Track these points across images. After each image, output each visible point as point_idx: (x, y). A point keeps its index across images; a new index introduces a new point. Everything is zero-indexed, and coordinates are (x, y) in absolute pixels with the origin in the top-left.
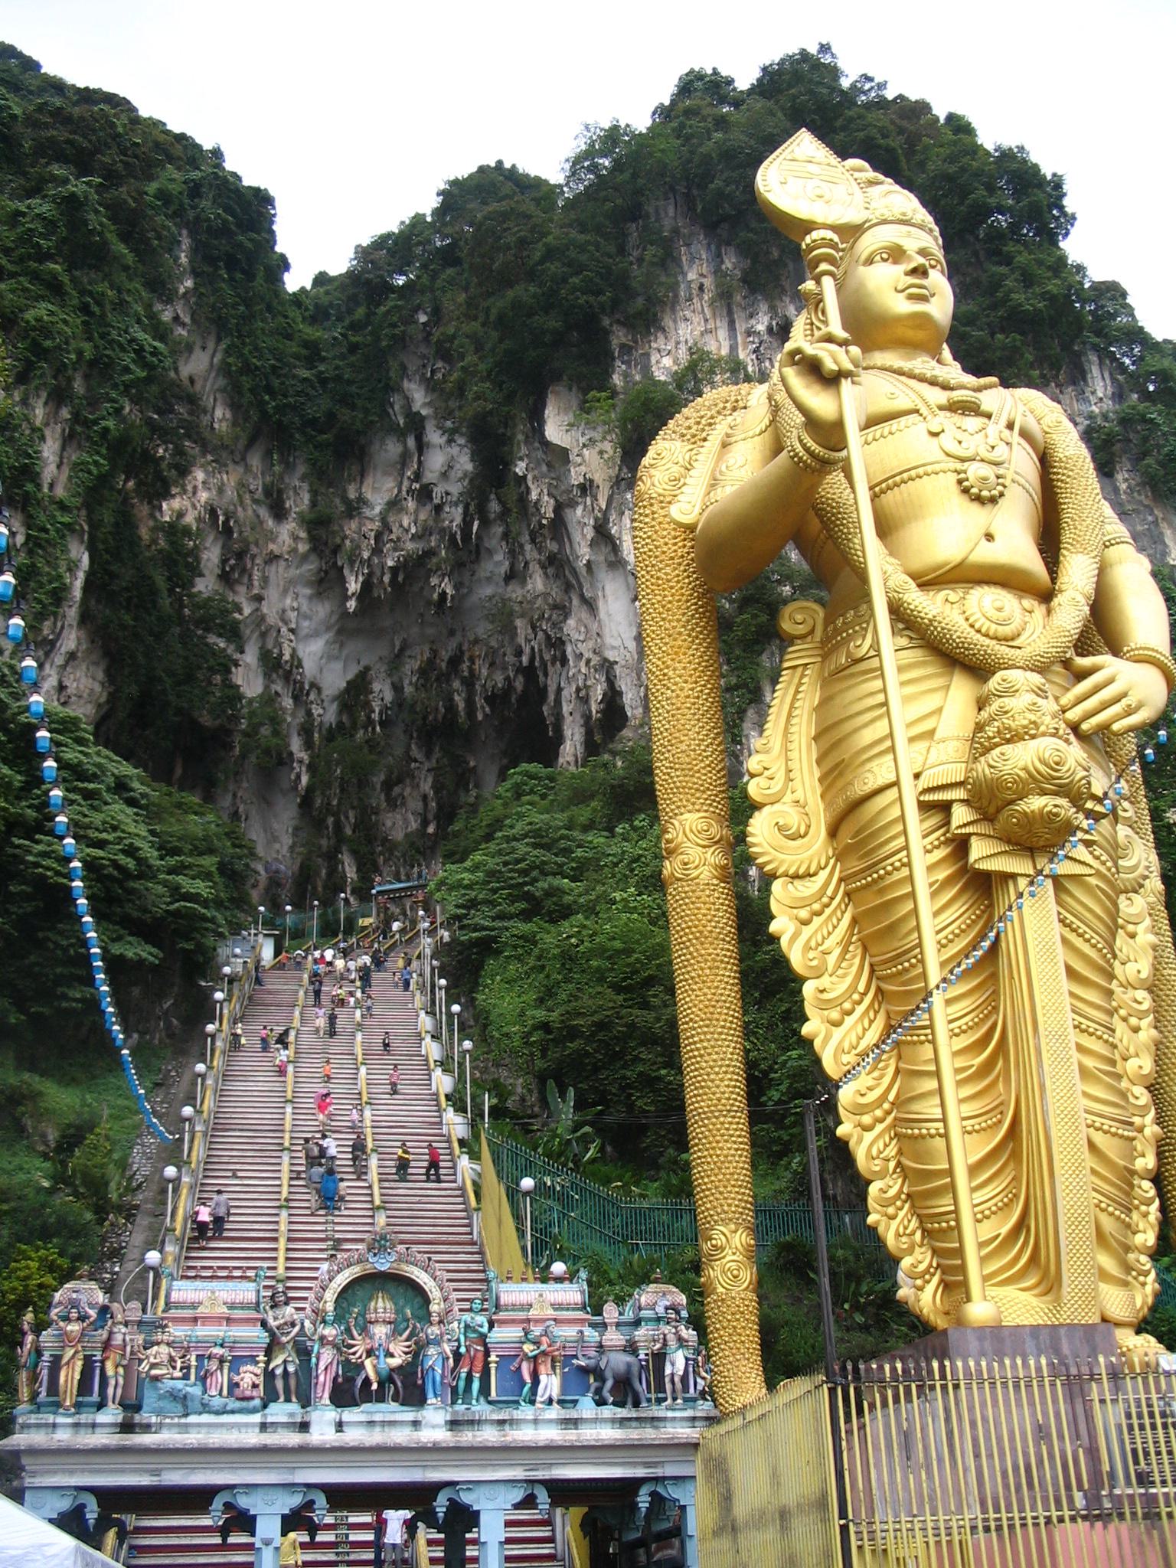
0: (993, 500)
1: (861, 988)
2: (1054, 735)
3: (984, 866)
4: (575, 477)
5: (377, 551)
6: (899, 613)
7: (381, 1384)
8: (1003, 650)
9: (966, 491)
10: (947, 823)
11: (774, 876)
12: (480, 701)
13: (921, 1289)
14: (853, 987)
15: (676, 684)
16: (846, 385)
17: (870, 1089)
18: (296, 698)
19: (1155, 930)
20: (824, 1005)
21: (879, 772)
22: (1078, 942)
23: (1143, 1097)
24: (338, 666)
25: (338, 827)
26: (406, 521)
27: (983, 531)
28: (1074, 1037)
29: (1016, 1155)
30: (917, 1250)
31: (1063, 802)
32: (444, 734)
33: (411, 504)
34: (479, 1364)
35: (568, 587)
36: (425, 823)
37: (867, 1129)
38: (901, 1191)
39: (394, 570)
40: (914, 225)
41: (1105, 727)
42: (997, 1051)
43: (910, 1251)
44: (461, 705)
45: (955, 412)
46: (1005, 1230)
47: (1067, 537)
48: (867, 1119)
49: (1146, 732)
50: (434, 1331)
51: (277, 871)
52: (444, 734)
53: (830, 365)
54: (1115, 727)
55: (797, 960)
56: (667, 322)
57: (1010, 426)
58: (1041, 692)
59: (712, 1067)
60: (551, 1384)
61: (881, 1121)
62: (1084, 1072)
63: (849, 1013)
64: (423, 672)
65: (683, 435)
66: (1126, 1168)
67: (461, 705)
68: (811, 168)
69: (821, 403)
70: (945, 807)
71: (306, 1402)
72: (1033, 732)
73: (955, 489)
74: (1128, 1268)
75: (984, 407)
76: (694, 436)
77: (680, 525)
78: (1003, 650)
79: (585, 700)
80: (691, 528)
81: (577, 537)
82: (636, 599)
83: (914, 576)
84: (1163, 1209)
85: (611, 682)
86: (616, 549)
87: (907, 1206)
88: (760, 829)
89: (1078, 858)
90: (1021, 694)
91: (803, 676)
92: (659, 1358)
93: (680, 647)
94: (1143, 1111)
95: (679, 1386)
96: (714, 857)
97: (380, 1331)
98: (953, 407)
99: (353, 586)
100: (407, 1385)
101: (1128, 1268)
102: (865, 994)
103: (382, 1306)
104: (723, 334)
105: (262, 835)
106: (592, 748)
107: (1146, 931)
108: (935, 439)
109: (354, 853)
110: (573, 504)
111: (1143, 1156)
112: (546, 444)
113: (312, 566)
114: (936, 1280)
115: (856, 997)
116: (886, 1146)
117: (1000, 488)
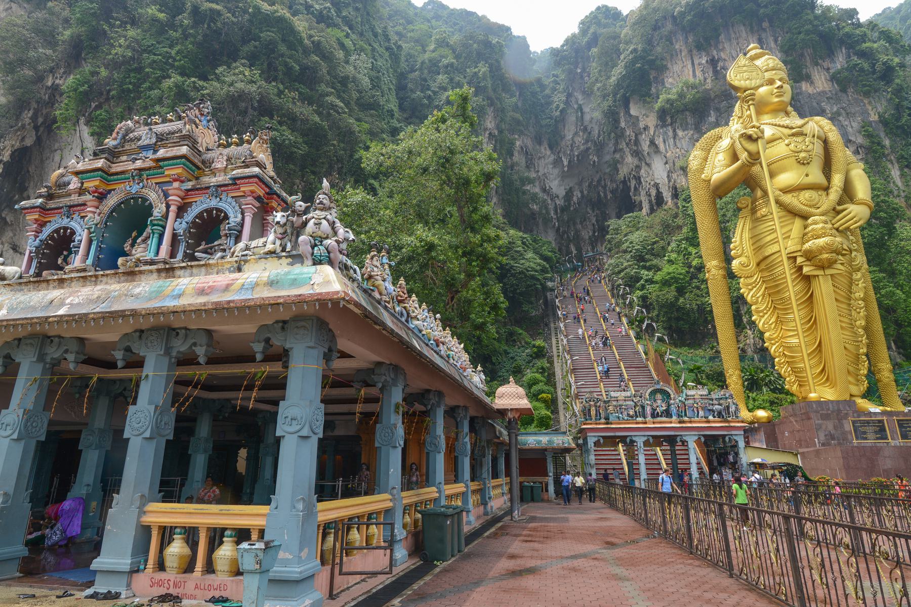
0: (808, 163)
4: (641, 125)
5: (572, 150)
6: (777, 202)
8: (813, 210)
10: (795, 261)
12: (608, 193)
14: (767, 306)
16: (760, 141)
18: (551, 200)
20: (758, 312)
21: (774, 248)
24: (563, 188)
25: (568, 237)
26: (579, 140)
28: (838, 318)
29: (820, 351)
31: (834, 255)
32: (599, 204)
33: (581, 134)
35: (640, 160)
36: (594, 232)
39: (578, 156)
41: (848, 229)
44: (602, 195)
47: (833, 168)
49: (862, 229)
50: (672, 402)
52: (599, 204)
53: (755, 136)
55: (749, 299)
56: (669, 66)
57: (814, 136)
58: (826, 222)
60: (701, 413)
62: (842, 328)
64: (589, 186)
67: (602, 195)
68: (745, 68)
70: (795, 258)
71: (645, 417)
74: (858, 381)
78: (813, 210)
79: (650, 196)
81: (643, 143)
82: (666, 163)
83: (781, 190)
84: (869, 363)
85: (658, 189)
86: (657, 147)
88: (735, 264)
90: (817, 223)
92: (728, 407)
94: (862, 336)
97: (659, 402)
98: (793, 135)
99: (566, 163)
100: (667, 413)
101: (858, 381)
103: (659, 396)
104: (690, 66)
106: (652, 210)
109: (574, 245)
110: (641, 133)
112: (631, 116)
113: (552, 158)
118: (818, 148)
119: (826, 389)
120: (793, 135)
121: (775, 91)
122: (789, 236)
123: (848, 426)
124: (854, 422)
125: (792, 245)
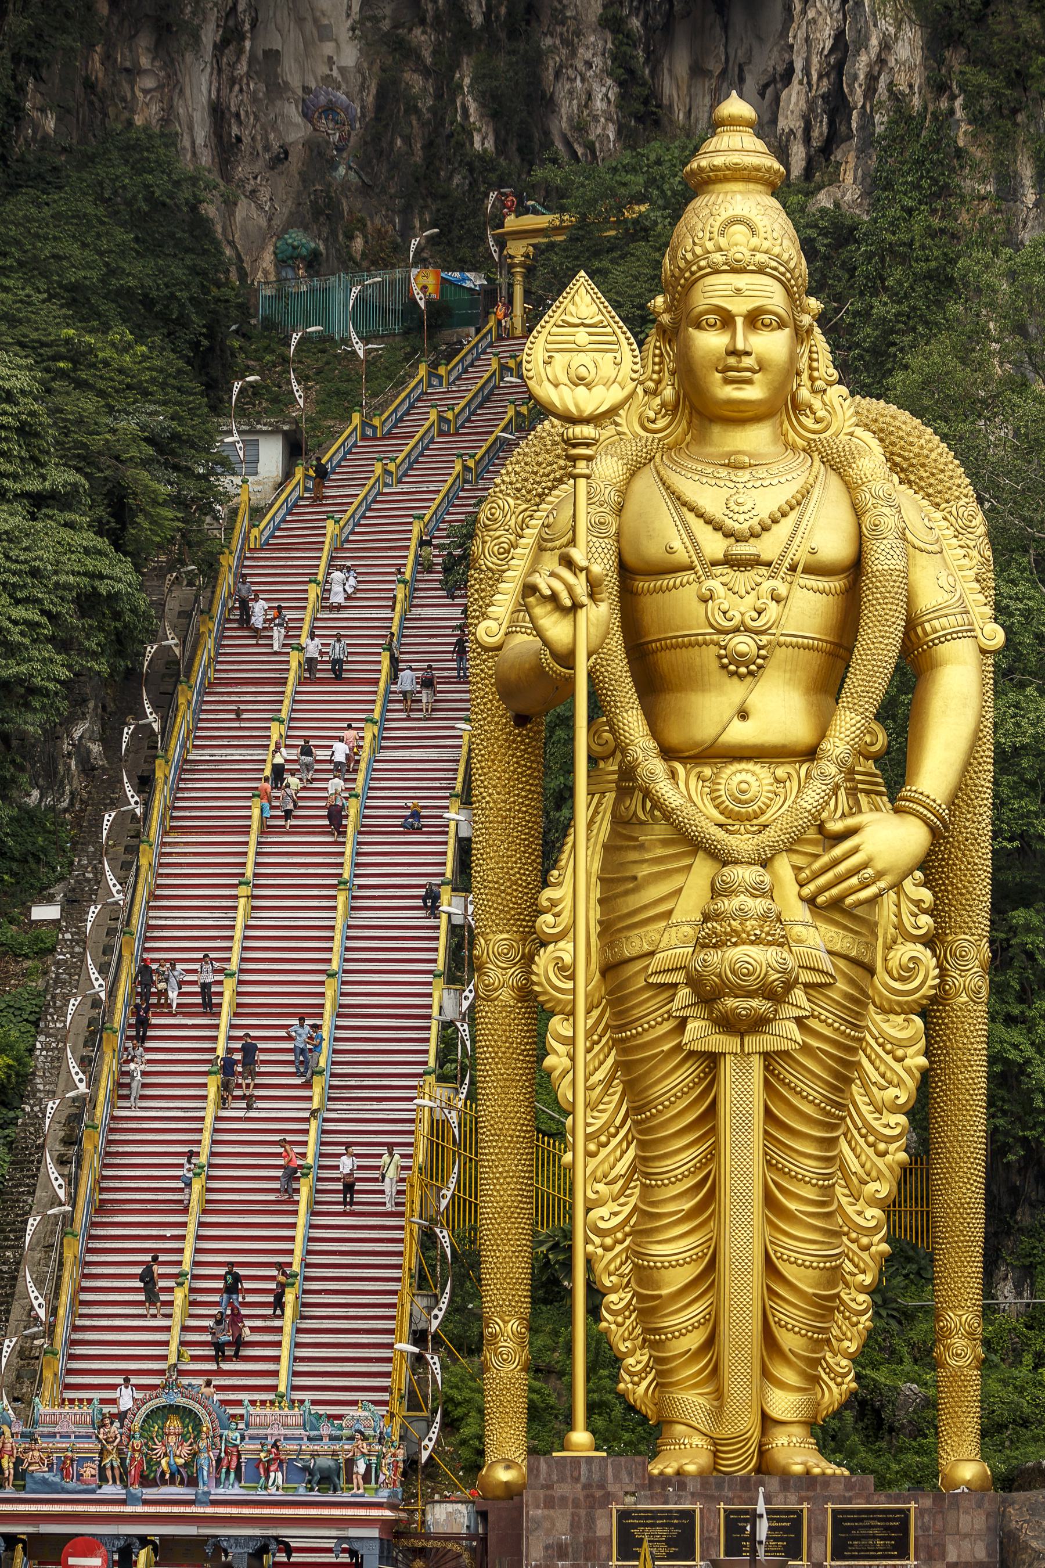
0: (751, 673)
1: (617, 1123)
2: (752, 943)
3: (697, 1047)
7: (172, 1475)
9: (724, 667)
11: (552, 1014)
13: (638, 1384)
15: (490, 795)
16: (582, 614)
17: (616, 1214)
19: (927, 1054)
22: (795, 1101)
23: (873, 1215)
27: (734, 710)
30: (638, 1352)
31: (755, 1003)
34: (234, 1465)
37: (607, 1249)
38: (630, 1303)
40: (752, 272)
41: (836, 904)
42: (708, 1196)
43: (631, 1353)
45: (732, 566)
46: (694, 1347)
48: (608, 1241)
50: (202, 1444)
51: (330, 109)
54: (849, 901)
57: (793, 568)
59: (498, 1179)
61: (622, 1242)
63: (605, 1145)
65: (518, 490)
66: (815, 1295)
68: (582, 336)
69: (557, 629)
72: (734, 940)
73: (714, 664)
75: (765, 557)
76: (529, 492)
77: (486, 649)
80: (499, 648)
87: (634, 1316)
89: (786, 1034)
91: (599, 803)
92: (350, 1463)
93: (496, 754)
95: (361, 1482)
96: (513, 976)
98: (731, 562)
102: (618, 1129)
103: (174, 1424)
105: (294, 34)
107: (917, 1054)
108: (704, 605)
111: (864, 1272)
114: (650, 1377)
115: (612, 1130)
116: (622, 1264)
117: (760, 661)
118: (808, 610)
119: (701, 1400)
120: (731, 562)
121: (732, 361)
122: (669, 913)
123: (607, 1526)
124: (623, 1515)
125: (671, 944)
